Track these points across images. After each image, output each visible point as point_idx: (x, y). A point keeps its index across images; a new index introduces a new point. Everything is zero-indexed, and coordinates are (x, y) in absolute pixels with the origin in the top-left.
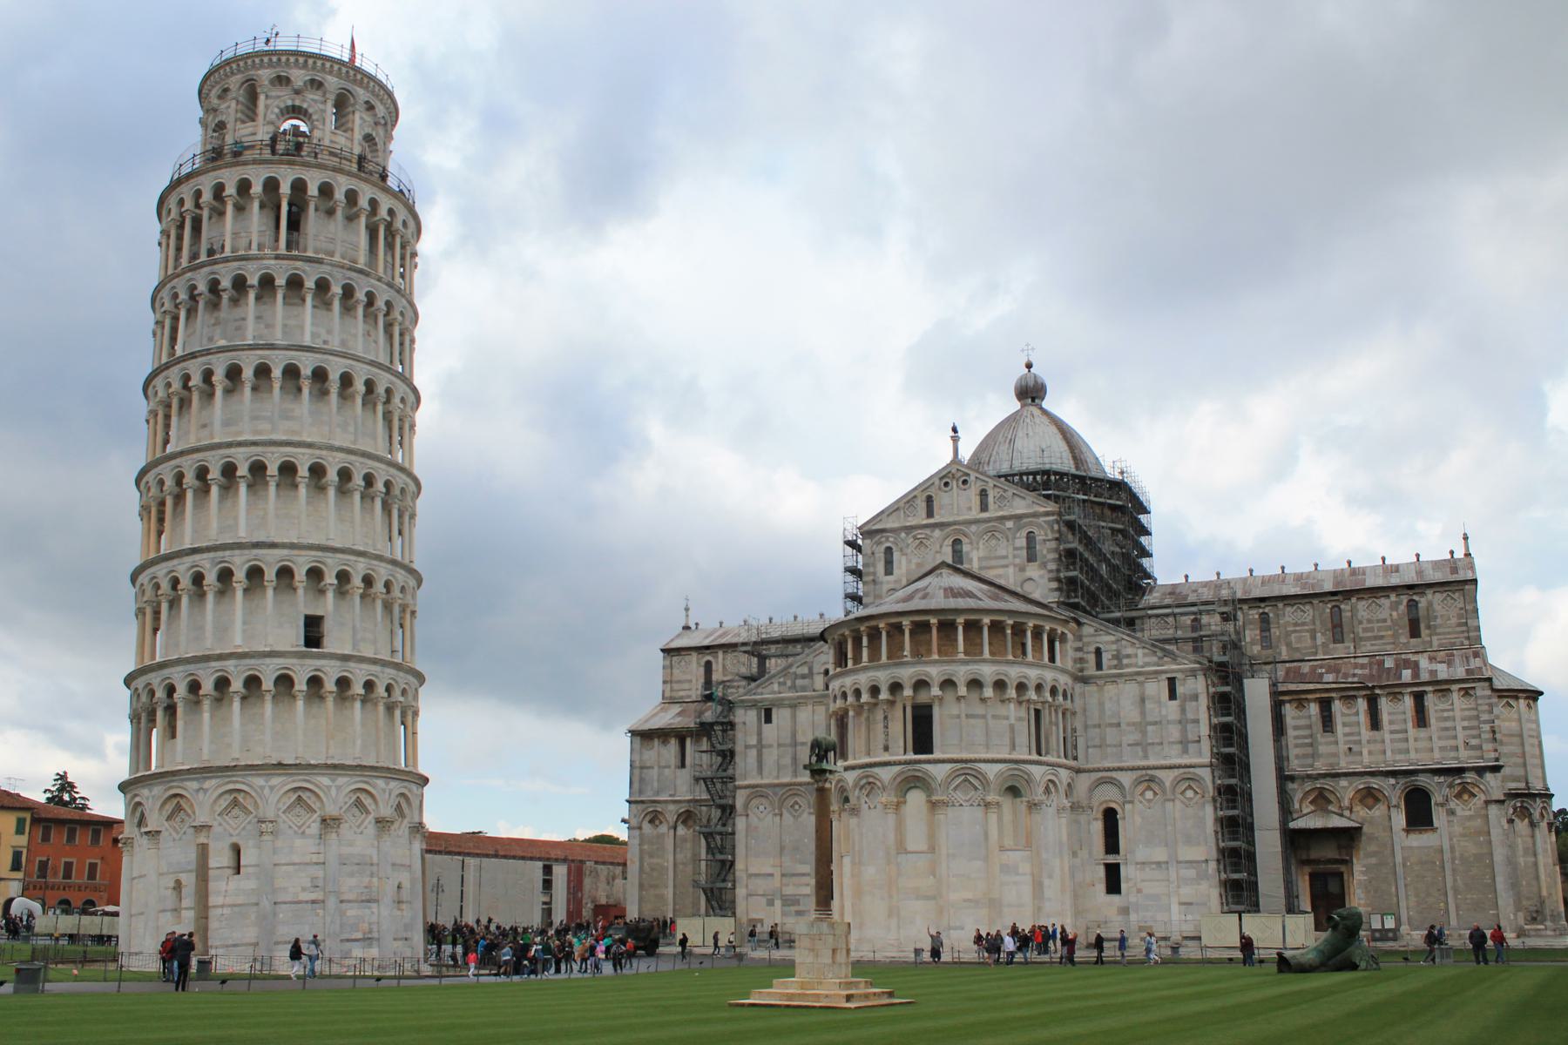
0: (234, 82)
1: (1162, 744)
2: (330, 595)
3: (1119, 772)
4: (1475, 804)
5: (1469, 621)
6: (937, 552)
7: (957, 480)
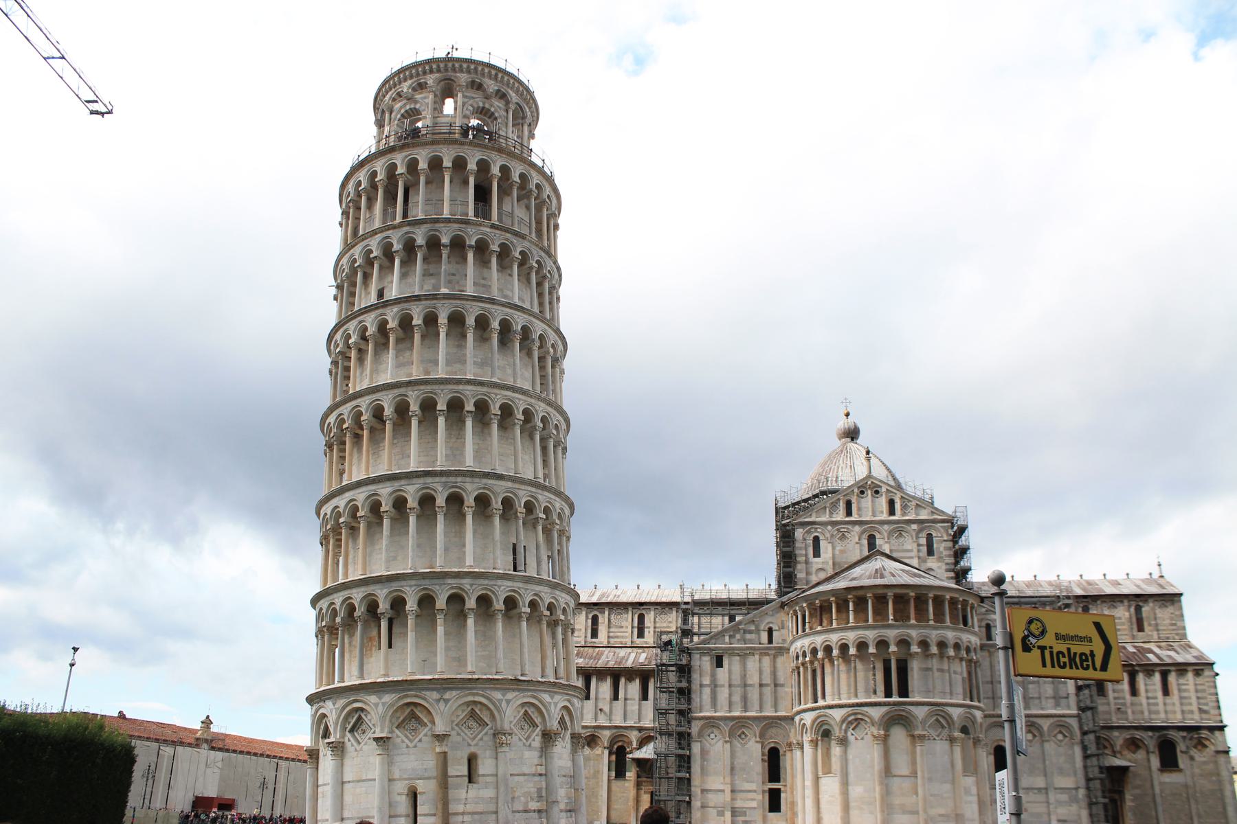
0: (431, 79)
1: (1039, 698)
6: (857, 543)
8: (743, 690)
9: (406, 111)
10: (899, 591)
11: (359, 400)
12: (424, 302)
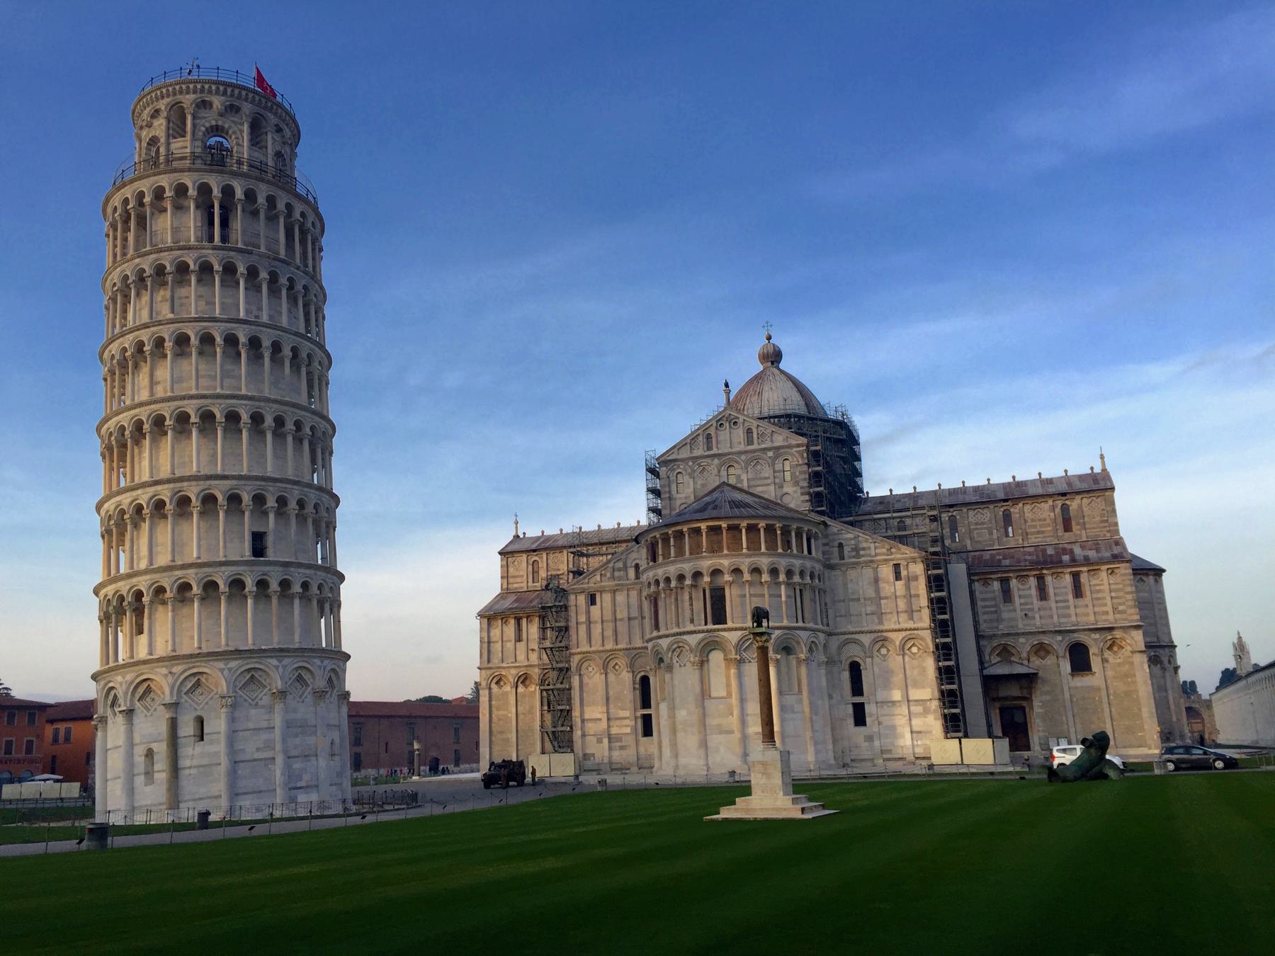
0: (162, 105)
2: (272, 516)
3: (861, 635)
4: (1123, 654)
5: (1109, 519)
7: (730, 422)
8: (614, 624)
9: (150, 139)
11: (110, 422)
12: (152, 329)
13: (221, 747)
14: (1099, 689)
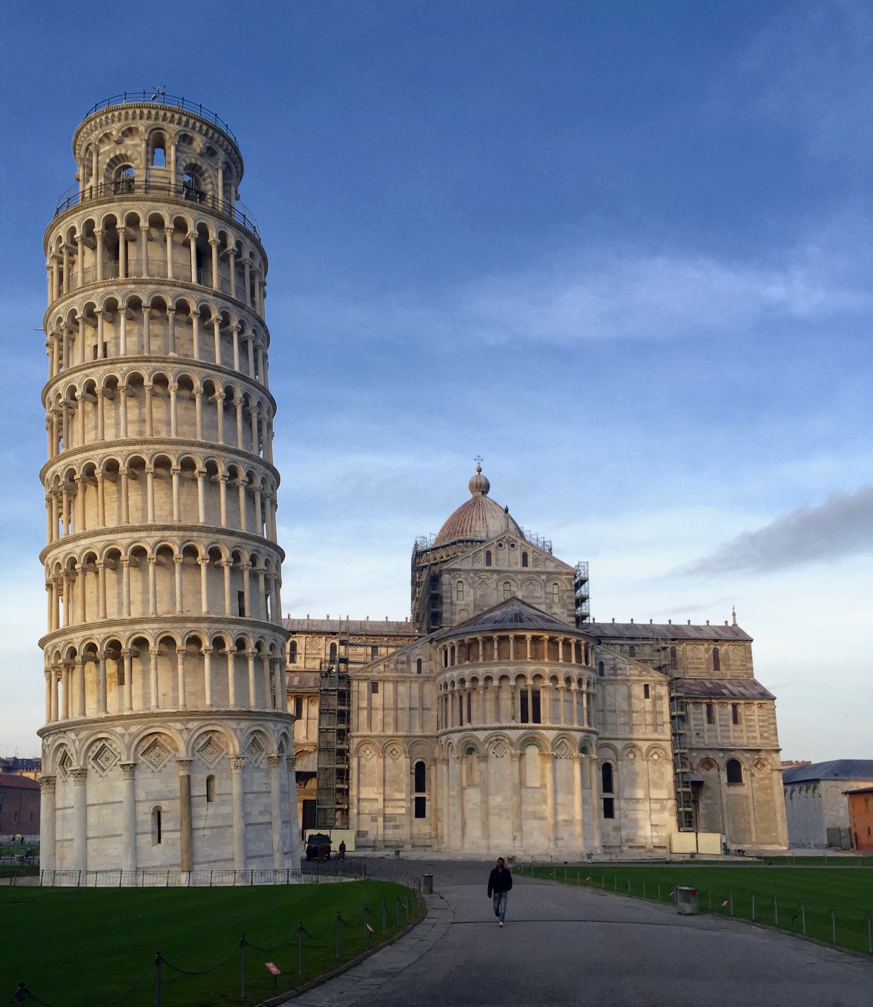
10: (535, 634)
13: (235, 809)
14: (747, 797)
